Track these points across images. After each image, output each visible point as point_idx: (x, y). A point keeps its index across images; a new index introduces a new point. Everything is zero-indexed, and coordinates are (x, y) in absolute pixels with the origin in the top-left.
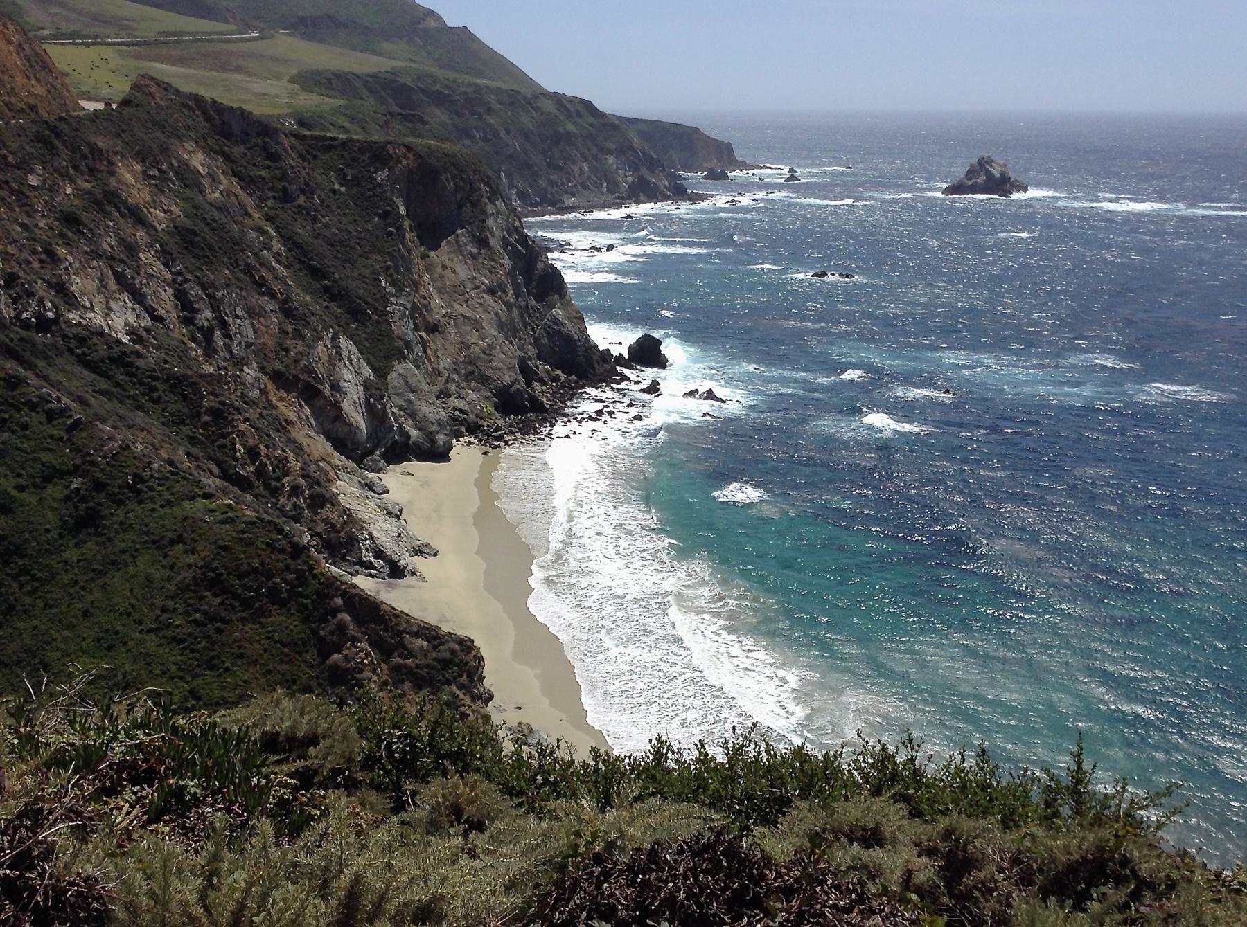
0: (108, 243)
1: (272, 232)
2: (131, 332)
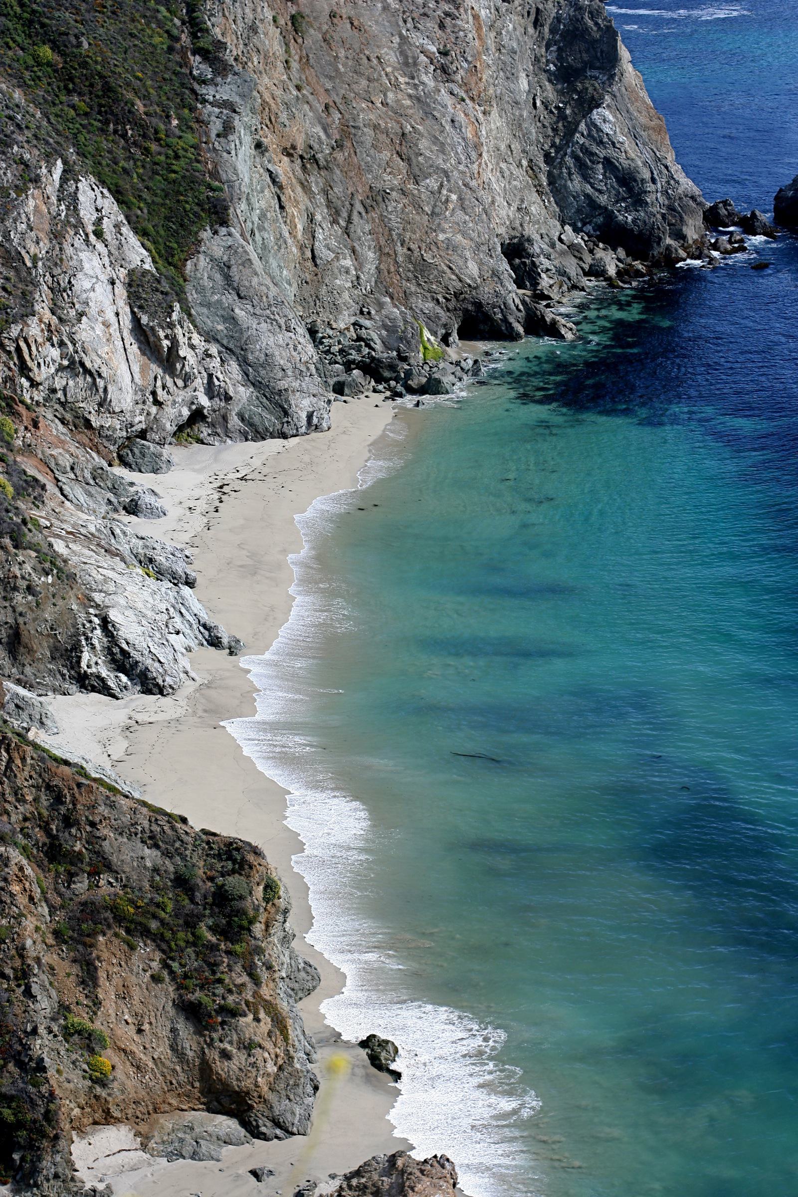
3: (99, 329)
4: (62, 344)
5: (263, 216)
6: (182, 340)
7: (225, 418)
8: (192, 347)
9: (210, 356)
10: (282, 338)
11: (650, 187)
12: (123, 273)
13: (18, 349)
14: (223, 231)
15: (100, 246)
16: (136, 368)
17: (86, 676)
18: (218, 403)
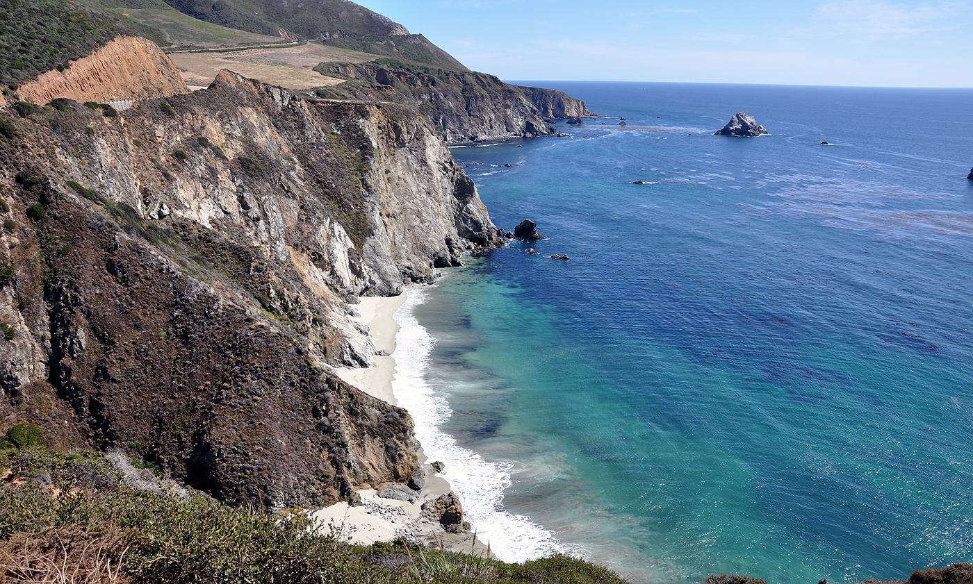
0: (200, 170)
2: (212, 221)
6: (363, 268)
8: (365, 269)
10: (389, 267)
12: (347, 249)
14: (372, 237)
15: (340, 241)
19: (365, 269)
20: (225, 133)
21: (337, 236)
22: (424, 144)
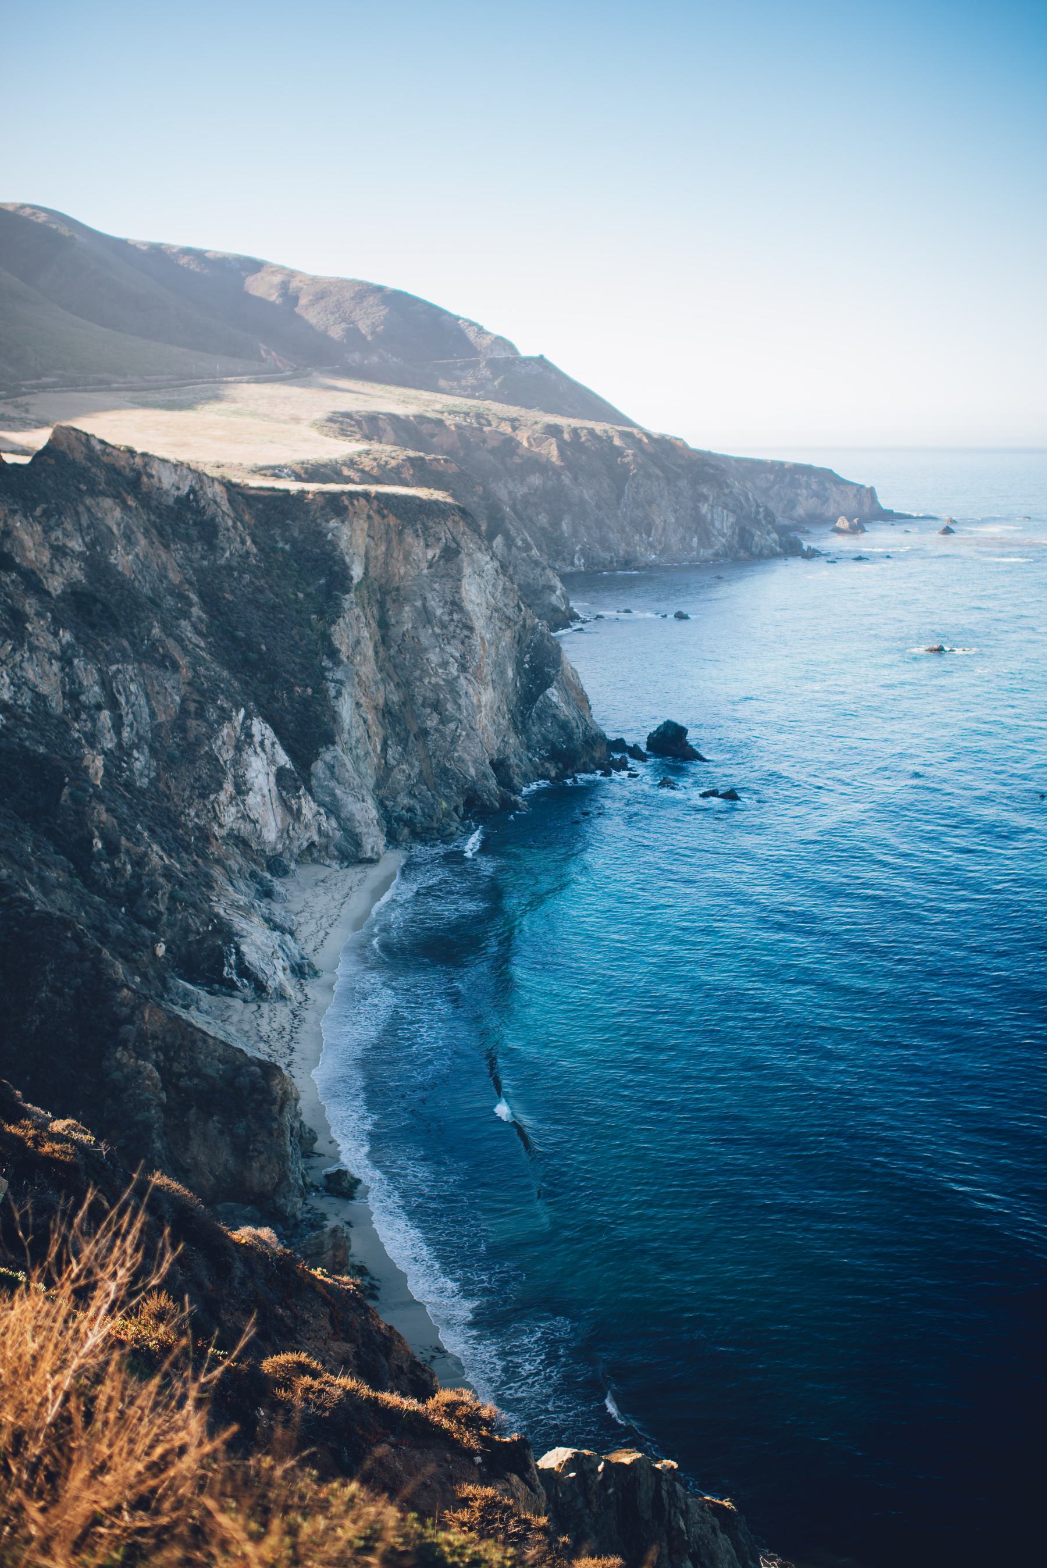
1: (194, 598)
3: (259, 798)
4: (237, 805)
5: (358, 741)
7: (327, 847)
9: (321, 814)
10: (359, 805)
11: (576, 730)
12: (274, 769)
13: (213, 808)
14: (332, 748)
15: (262, 754)
16: (279, 819)
17: (225, 979)
18: (324, 840)
19: (308, 808)
20: (52, 547)
21: (257, 745)
22: (460, 571)
